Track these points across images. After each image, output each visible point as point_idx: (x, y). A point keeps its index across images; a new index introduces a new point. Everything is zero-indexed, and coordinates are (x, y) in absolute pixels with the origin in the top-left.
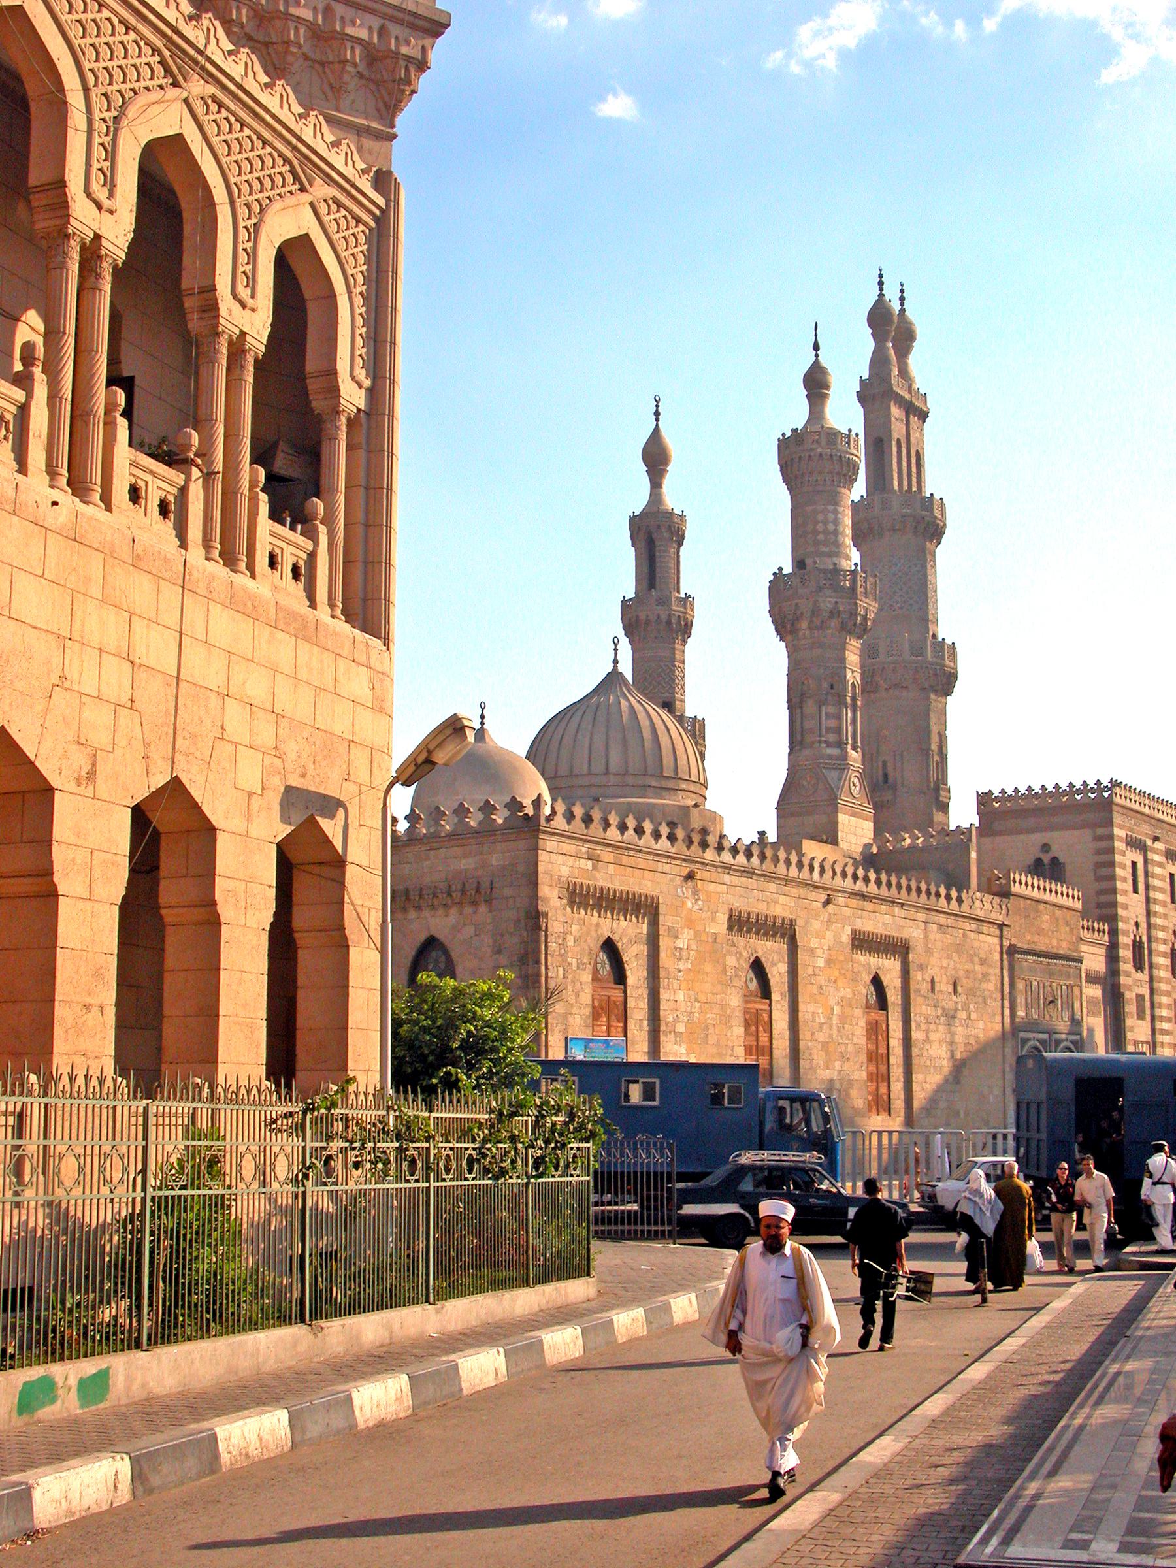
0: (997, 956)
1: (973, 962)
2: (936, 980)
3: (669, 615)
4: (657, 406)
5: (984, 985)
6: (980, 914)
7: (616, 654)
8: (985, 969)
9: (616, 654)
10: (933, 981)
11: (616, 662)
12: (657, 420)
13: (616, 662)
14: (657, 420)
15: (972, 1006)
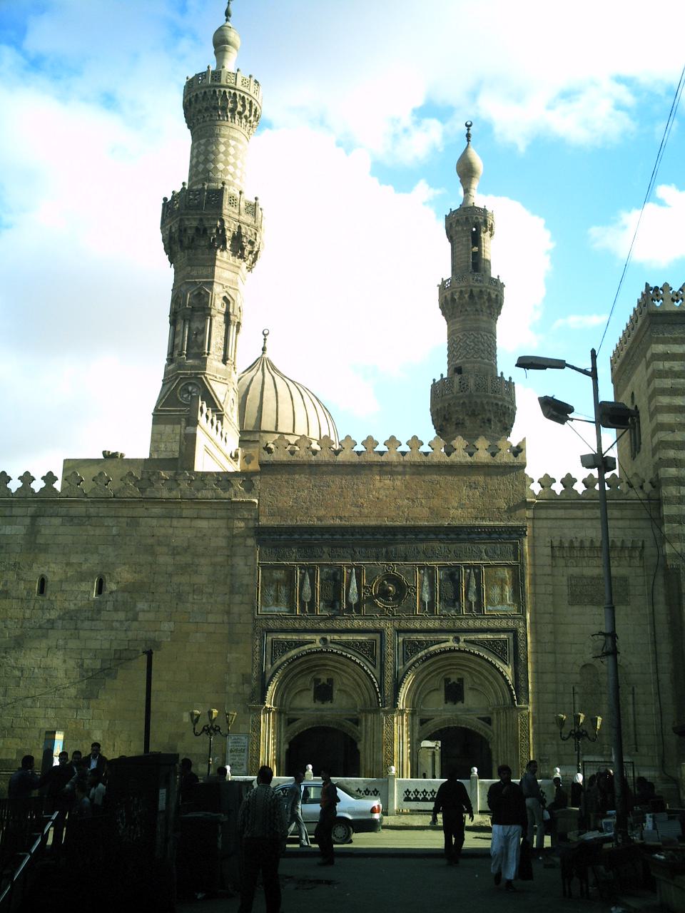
0: (221, 542)
1: (154, 554)
2: (49, 577)
3: (452, 293)
4: (468, 130)
5: (184, 579)
6: (165, 494)
7: (265, 343)
8: (182, 559)
9: (265, 343)
10: (43, 582)
11: (264, 349)
12: (468, 141)
13: (264, 349)
14: (468, 141)
15: (141, 605)
